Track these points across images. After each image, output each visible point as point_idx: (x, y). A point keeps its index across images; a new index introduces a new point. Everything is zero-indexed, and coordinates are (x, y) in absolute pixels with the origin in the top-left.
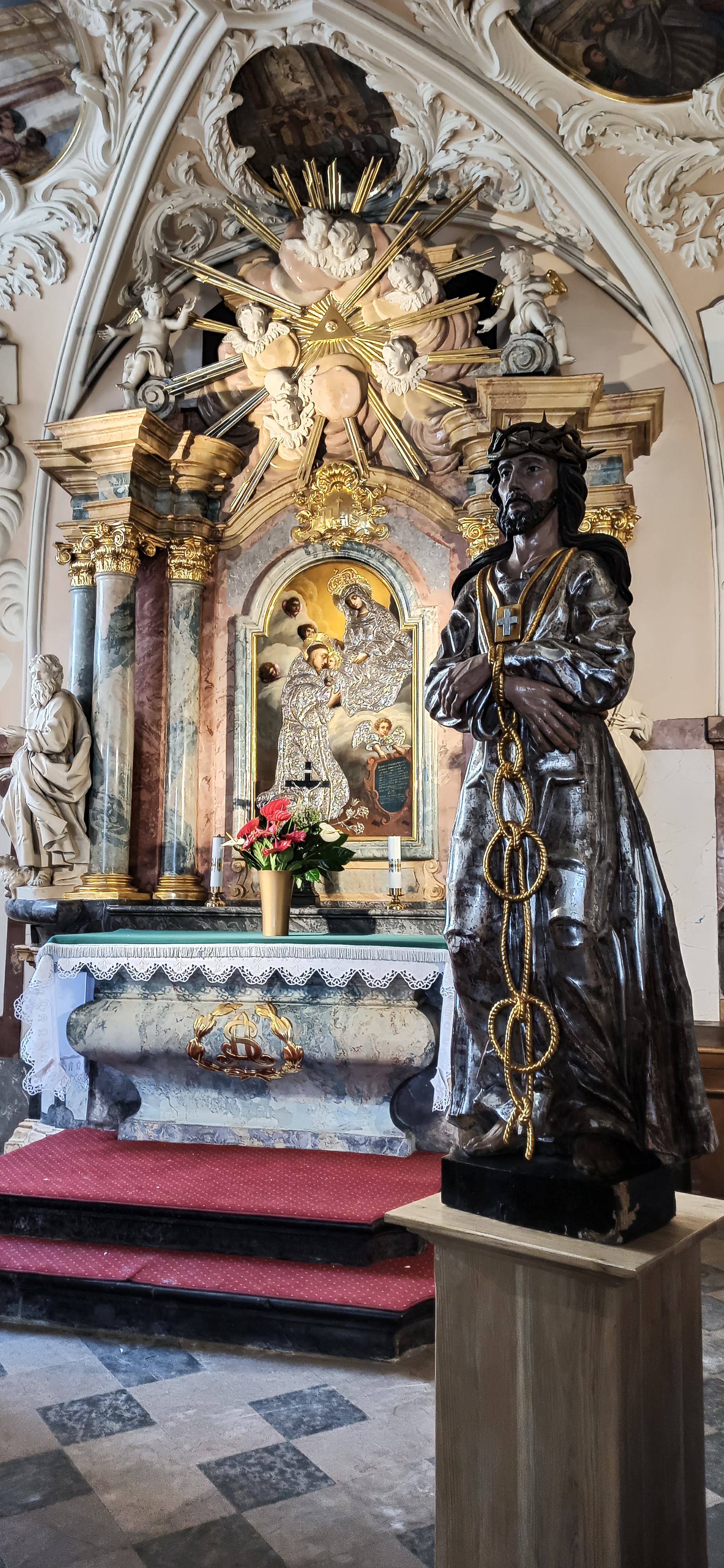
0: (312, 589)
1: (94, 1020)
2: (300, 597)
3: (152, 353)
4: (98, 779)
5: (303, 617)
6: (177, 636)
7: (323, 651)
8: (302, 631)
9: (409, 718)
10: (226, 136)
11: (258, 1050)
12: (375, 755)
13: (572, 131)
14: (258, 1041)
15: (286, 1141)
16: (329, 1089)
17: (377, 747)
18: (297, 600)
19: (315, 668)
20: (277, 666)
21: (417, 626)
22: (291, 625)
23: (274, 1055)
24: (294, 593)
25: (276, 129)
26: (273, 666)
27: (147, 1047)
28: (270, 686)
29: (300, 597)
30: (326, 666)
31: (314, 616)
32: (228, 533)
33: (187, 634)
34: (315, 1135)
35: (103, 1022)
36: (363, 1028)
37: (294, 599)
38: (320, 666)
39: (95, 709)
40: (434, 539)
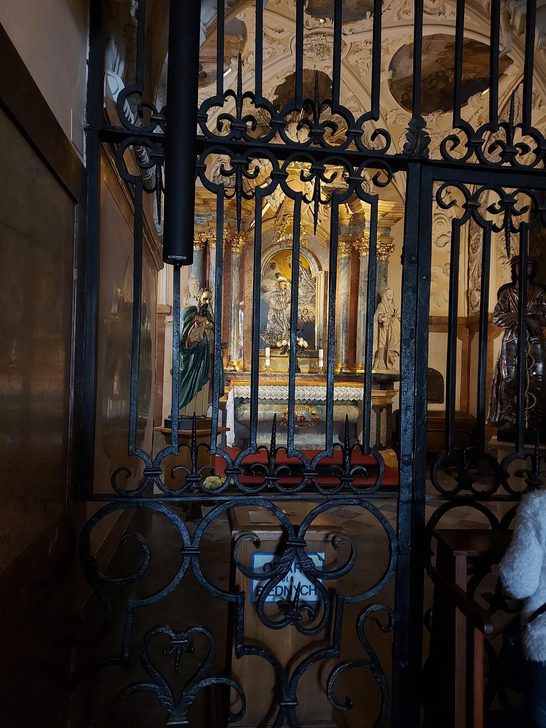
0: (281, 260)
2: (276, 262)
5: (277, 270)
6: (235, 273)
7: (284, 283)
8: (277, 275)
10: (274, 91)
11: (304, 418)
13: (391, 117)
14: (305, 416)
15: (307, 448)
16: (320, 431)
19: (281, 289)
22: (273, 272)
23: (310, 420)
24: (274, 261)
25: (289, 92)
27: (265, 419)
29: (276, 262)
30: (285, 288)
31: (281, 270)
32: (249, 236)
33: (238, 273)
34: (317, 445)
37: (274, 263)
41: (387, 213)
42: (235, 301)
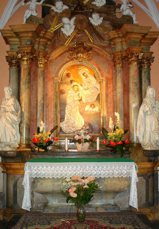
1: (39, 183)
3: (33, 10)
4: (23, 119)
6: (40, 82)
9: (99, 104)
12: (91, 113)
17: (91, 111)
18: (70, 73)
19: (75, 91)
20: (65, 90)
21: (101, 82)
26: (63, 90)
28: (63, 95)
31: (74, 78)
35: (42, 183)
36: (112, 182)
38: (76, 90)
39: (21, 100)
40: (104, 60)
41: (146, 34)
42: (41, 101)
